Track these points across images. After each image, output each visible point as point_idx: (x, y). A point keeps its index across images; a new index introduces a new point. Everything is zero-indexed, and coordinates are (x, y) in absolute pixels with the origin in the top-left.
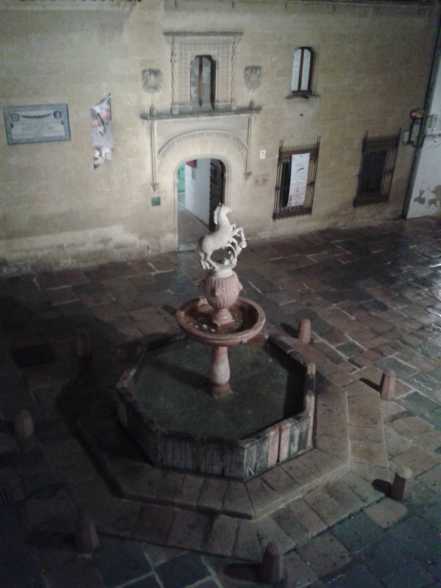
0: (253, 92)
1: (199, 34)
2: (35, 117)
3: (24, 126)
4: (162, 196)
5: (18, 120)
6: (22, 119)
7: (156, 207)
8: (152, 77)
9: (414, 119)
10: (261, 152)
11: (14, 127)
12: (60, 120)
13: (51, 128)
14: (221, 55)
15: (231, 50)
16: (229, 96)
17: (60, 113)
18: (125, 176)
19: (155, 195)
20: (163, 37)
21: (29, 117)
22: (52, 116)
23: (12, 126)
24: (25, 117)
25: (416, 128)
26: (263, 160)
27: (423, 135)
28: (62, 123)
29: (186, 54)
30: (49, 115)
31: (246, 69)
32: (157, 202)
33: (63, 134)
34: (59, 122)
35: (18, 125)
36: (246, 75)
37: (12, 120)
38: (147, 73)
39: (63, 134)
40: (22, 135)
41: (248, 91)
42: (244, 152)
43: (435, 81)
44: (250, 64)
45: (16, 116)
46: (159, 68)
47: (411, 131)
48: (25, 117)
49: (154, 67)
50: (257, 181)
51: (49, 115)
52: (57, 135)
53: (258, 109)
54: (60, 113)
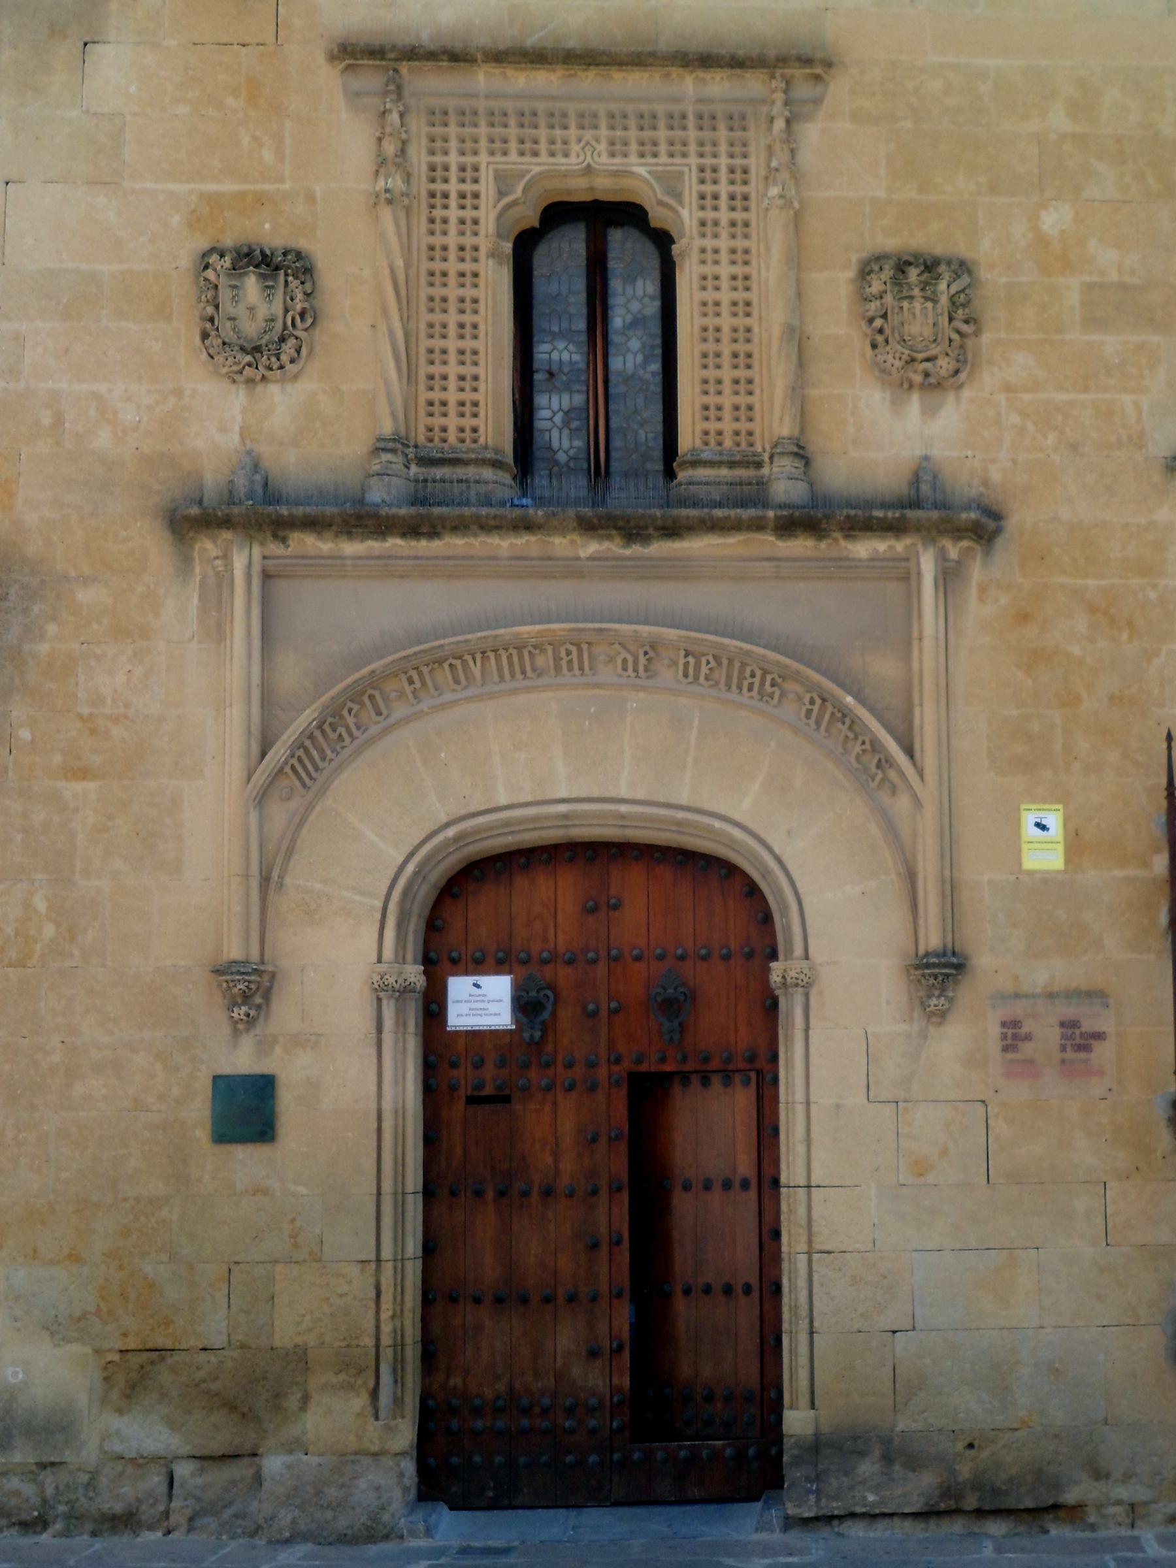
0: (929, 412)
1: (537, 58)
4: (293, 1072)
7: (241, 1153)
8: (251, 284)
10: (1029, 819)
14: (691, 187)
18: (41, 904)
19: (243, 1060)
20: (328, 78)
26: (1046, 879)
29: (468, 173)
31: (865, 272)
32: (247, 1111)
41: (897, 404)
44: (890, 243)
46: (302, 244)
49: (271, 234)
50: (1013, 1036)
53: (982, 525)
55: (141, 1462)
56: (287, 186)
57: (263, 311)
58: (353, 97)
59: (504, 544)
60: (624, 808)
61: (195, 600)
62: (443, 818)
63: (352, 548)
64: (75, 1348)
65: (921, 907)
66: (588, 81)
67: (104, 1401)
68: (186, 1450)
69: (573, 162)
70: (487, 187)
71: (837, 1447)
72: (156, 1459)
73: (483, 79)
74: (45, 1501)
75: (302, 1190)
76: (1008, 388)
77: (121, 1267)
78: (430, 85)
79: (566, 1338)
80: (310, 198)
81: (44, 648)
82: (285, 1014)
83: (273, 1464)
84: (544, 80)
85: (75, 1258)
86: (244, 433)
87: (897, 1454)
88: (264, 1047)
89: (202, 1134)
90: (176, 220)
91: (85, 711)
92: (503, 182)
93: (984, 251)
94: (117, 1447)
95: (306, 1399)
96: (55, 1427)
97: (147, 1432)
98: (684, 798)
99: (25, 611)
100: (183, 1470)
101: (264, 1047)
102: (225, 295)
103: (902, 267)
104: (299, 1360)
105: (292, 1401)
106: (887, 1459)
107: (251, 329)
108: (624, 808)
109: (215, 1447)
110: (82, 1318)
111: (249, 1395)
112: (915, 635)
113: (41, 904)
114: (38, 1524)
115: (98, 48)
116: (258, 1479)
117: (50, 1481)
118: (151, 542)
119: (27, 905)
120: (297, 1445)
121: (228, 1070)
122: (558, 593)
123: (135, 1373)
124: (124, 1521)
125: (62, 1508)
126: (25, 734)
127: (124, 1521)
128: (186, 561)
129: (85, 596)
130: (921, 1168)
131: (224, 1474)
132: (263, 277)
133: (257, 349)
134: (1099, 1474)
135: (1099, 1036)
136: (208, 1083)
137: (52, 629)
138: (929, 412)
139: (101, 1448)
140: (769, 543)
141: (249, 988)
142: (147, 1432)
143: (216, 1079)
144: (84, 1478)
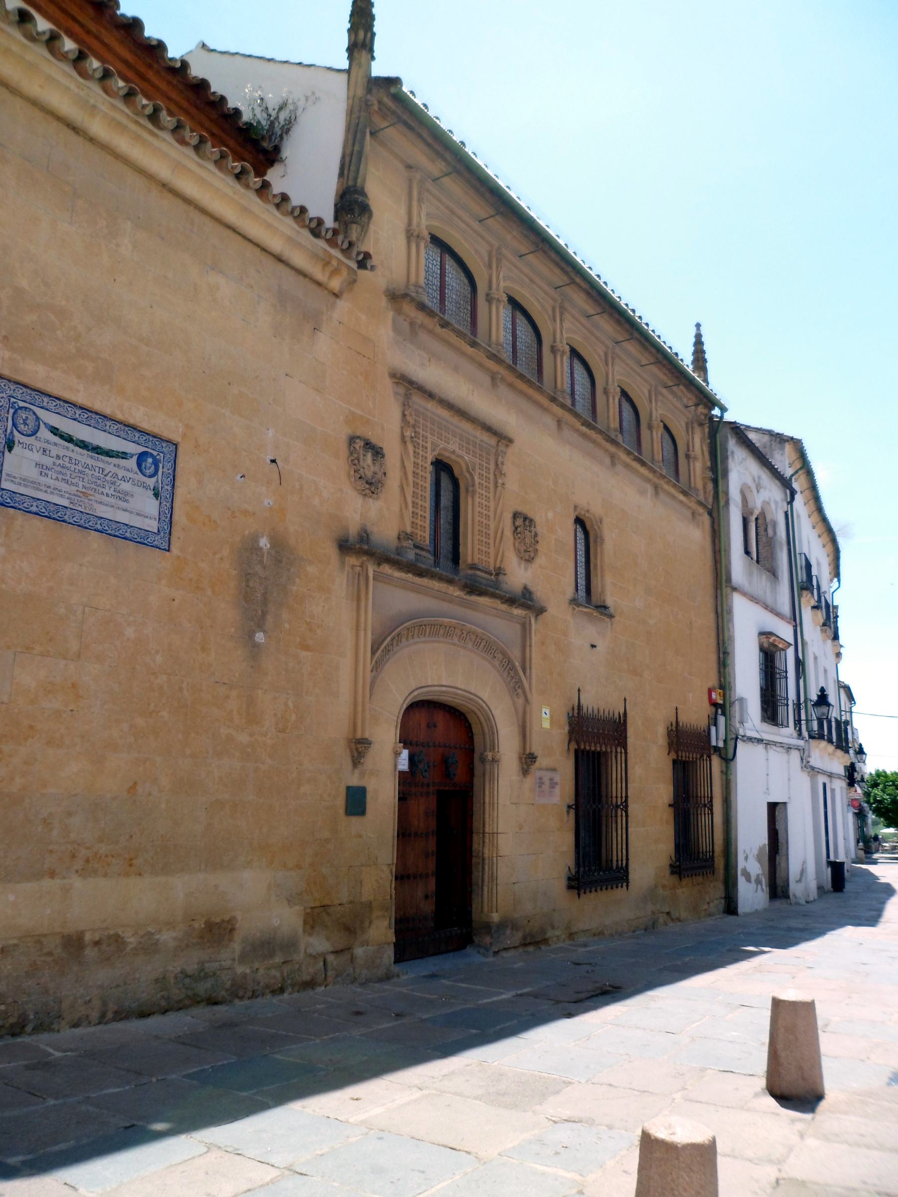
0: (526, 569)
2: (83, 445)
3: (47, 461)
4: (371, 785)
5: (34, 433)
6: (44, 433)
7: (354, 819)
9: (714, 704)
10: (544, 710)
11: (17, 449)
12: (151, 482)
13: (124, 496)
15: (492, 467)
16: (492, 560)
17: (156, 463)
18: (291, 705)
19: (355, 781)
20: (388, 382)
21: (69, 439)
22: (132, 463)
23: (10, 445)
24: (54, 431)
25: (721, 720)
27: (734, 736)
28: (156, 495)
30: (124, 455)
31: (516, 515)
32: (356, 801)
33: (152, 525)
34: (146, 488)
35: (29, 447)
36: (516, 528)
37: (14, 425)
38: (359, 444)
39: (152, 525)
40: (36, 486)
42: (520, 701)
43: (731, 639)
45: (31, 422)
47: (716, 725)
48: (54, 431)
51: (124, 455)
52: (137, 522)
54: (156, 463)
55: (314, 957)
56: (376, 420)
57: (372, 468)
58: (396, 393)
59: (436, 585)
60: (459, 692)
61: (345, 581)
62: (414, 687)
63: (398, 574)
64: (297, 908)
65: (528, 738)
66: (456, 420)
67: (304, 931)
68: (331, 949)
69: (451, 447)
70: (429, 445)
71: (503, 925)
72: (319, 955)
73: (431, 405)
74: (283, 979)
75: (372, 836)
76: (541, 567)
77: (314, 870)
78: (417, 400)
79: (420, 894)
80: (383, 428)
81: (294, 588)
82: (368, 762)
83: (359, 951)
84: (445, 414)
85: (299, 867)
86: (361, 514)
87: (515, 927)
88: (362, 775)
89: (342, 811)
90: (341, 417)
91: (308, 620)
92: (434, 446)
93: (537, 519)
94: (311, 951)
95: (370, 923)
96: (290, 945)
97: (319, 944)
98: (473, 691)
99: (288, 570)
100: (331, 958)
101: (362, 775)
102: (361, 457)
103: (525, 519)
104: (369, 906)
105: (367, 924)
106: (512, 929)
107: (369, 474)
108: (459, 692)
109: (340, 947)
110: (301, 894)
111: (351, 926)
112: (528, 644)
113: (291, 705)
114: (282, 990)
115: (318, 332)
116: (352, 959)
117: (286, 969)
118: (331, 551)
119: (286, 705)
120: (366, 943)
121: (350, 784)
122: (445, 606)
123: (314, 919)
124: (310, 984)
125: (289, 982)
126: (287, 626)
127: (310, 984)
128: (343, 563)
129: (311, 569)
130: (521, 828)
131: (347, 956)
132: (373, 455)
133: (370, 484)
134: (553, 928)
135: (556, 784)
136: (345, 789)
137: (297, 580)
138: (526, 569)
139: (306, 953)
140: (498, 604)
141: (359, 748)
142: (319, 944)
143: (348, 788)
144: (297, 966)
